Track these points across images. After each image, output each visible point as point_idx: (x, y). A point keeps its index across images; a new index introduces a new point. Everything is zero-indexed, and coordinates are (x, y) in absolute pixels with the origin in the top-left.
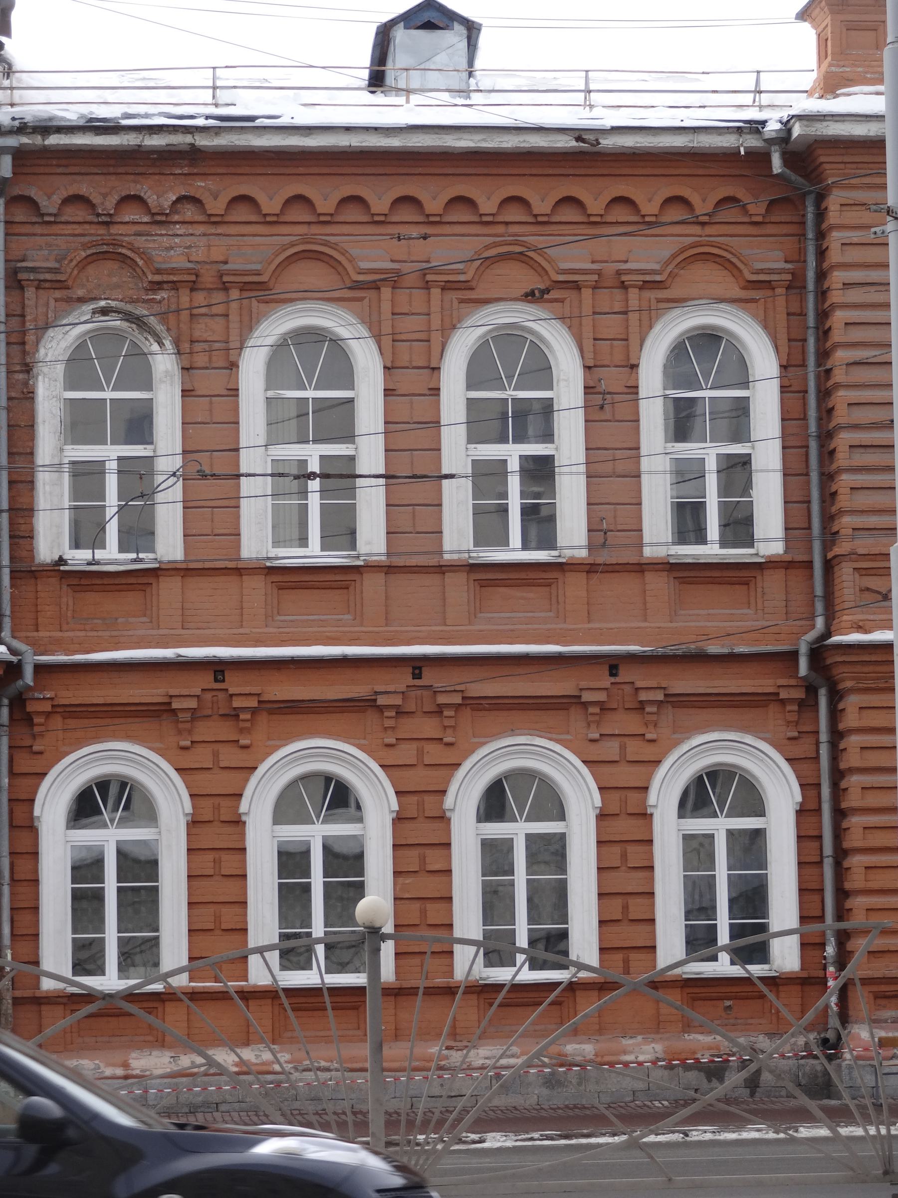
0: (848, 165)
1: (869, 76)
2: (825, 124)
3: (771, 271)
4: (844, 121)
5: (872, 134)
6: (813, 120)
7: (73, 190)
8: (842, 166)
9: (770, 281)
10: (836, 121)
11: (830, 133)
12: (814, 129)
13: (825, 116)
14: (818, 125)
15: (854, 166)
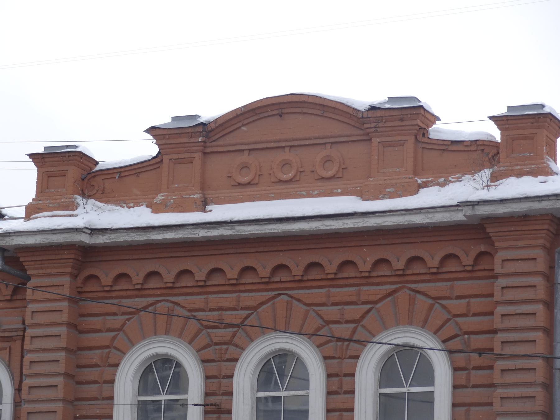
0: (36, 262)
1: (51, 205)
2: (11, 238)
3: (11, 330)
4: (22, 235)
5: (37, 242)
6: (5, 236)
7: (120, 271)
8: (33, 263)
9: (11, 337)
10: (18, 236)
11: (14, 244)
12: (5, 242)
13: (10, 233)
14: (7, 239)
15: (40, 262)
